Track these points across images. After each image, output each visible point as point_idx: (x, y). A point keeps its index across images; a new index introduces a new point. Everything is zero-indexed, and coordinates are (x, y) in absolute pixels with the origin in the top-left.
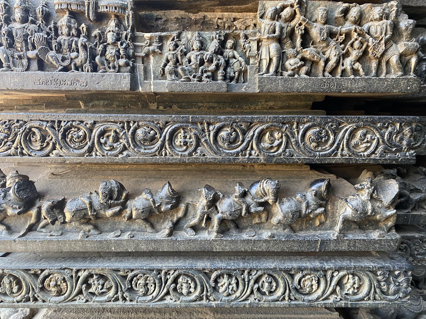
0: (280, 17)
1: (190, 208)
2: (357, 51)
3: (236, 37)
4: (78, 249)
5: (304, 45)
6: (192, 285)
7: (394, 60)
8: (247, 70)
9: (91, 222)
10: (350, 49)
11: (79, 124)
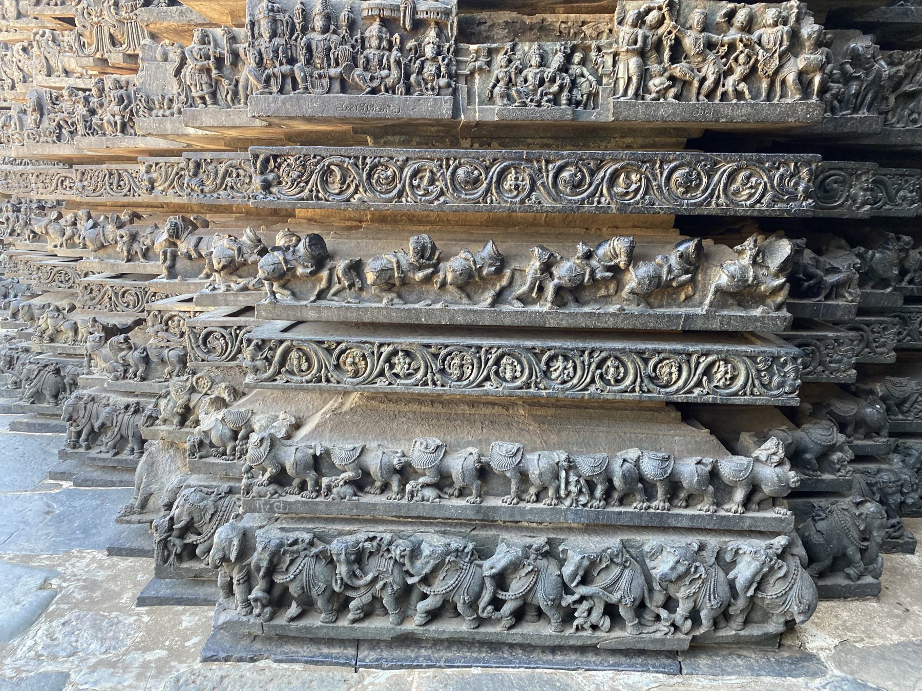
0: (644, 22)
1: (517, 275)
2: (743, 67)
3: (586, 50)
4: (382, 319)
5: (674, 59)
6: (518, 368)
7: (791, 78)
8: (598, 92)
9: (395, 289)
10: (733, 65)
11: (387, 161)
